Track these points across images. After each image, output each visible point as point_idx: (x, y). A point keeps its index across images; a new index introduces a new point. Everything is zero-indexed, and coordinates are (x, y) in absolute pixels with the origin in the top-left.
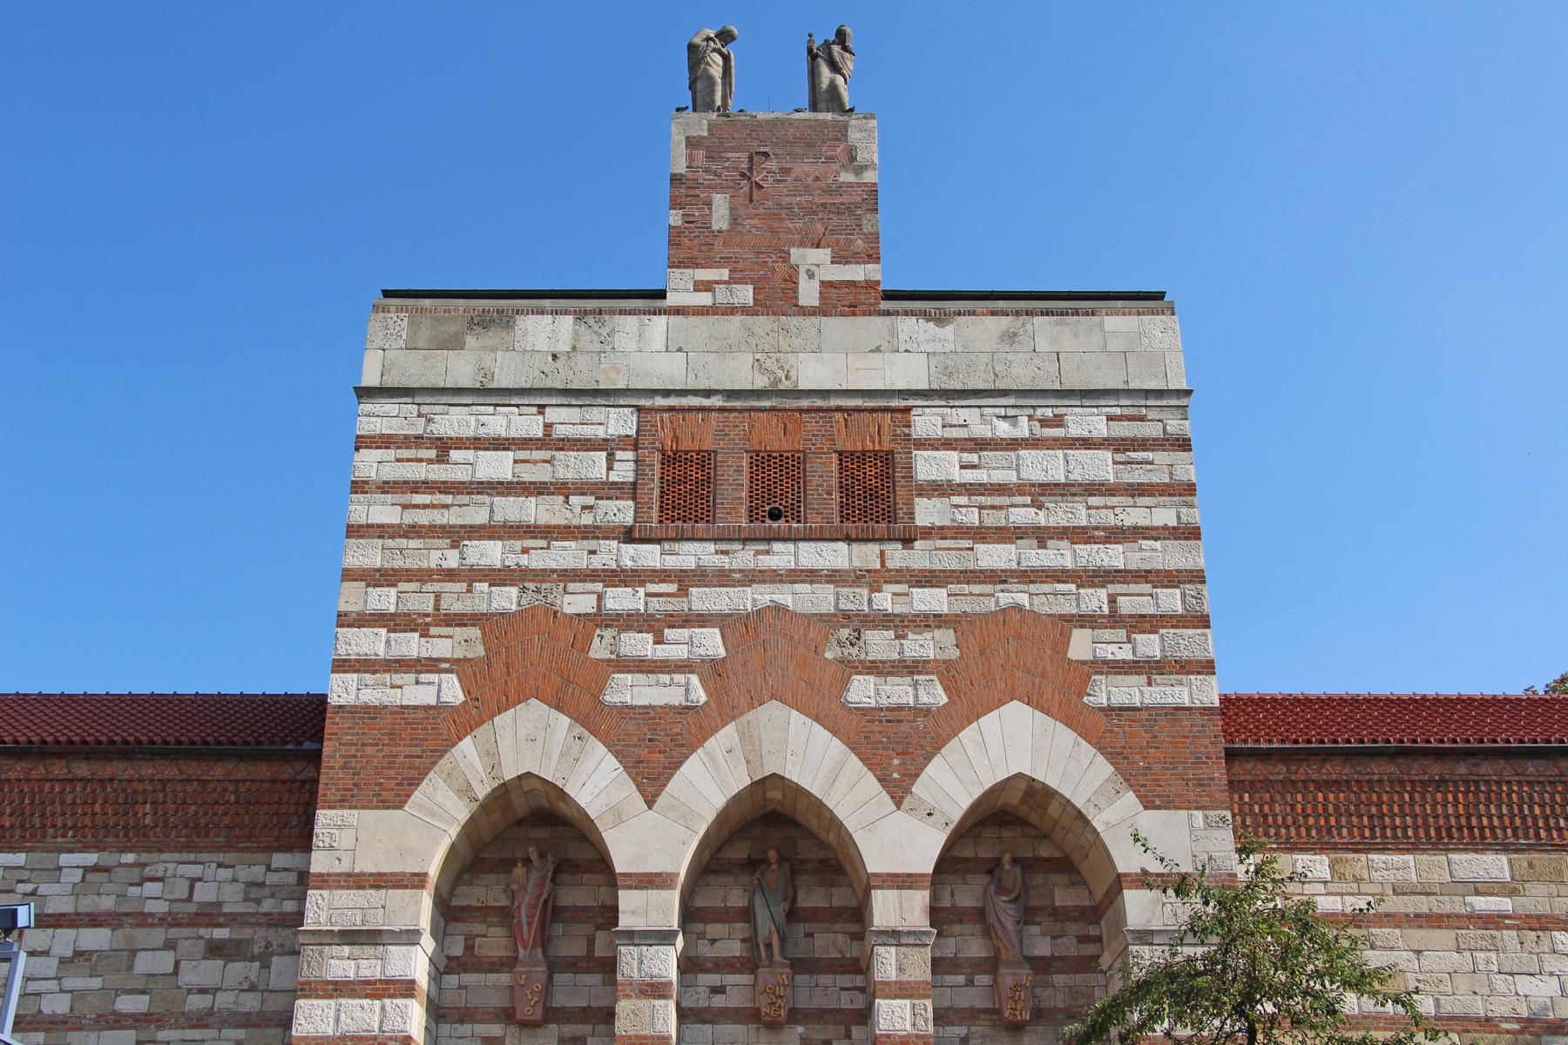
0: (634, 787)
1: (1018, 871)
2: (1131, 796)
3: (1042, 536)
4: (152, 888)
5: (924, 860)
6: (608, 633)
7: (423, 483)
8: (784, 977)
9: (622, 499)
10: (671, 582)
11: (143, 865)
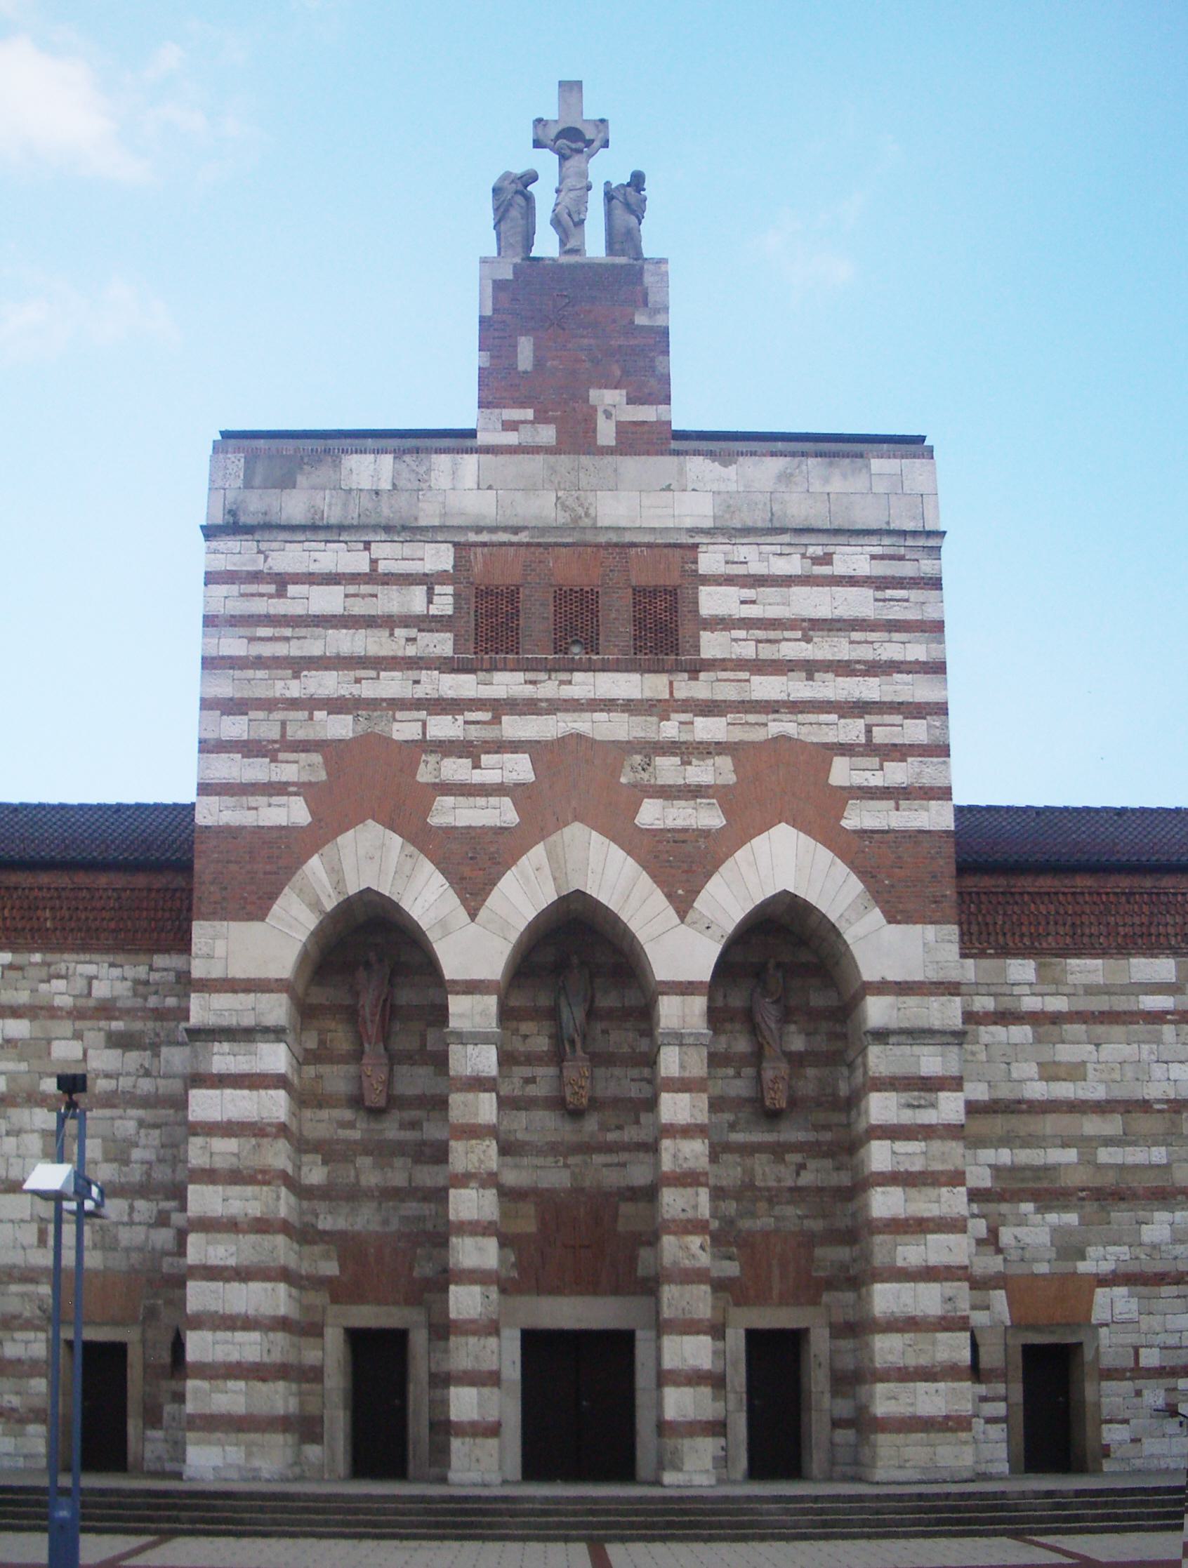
0: (458, 901)
1: (780, 974)
2: (877, 910)
3: (810, 668)
4: (59, 985)
5: (702, 968)
6: (432, 759)
7: (265, 616)
8: (585, 1069)
9: (442, 631)
10: (487, 710)
11: (49, 965)
